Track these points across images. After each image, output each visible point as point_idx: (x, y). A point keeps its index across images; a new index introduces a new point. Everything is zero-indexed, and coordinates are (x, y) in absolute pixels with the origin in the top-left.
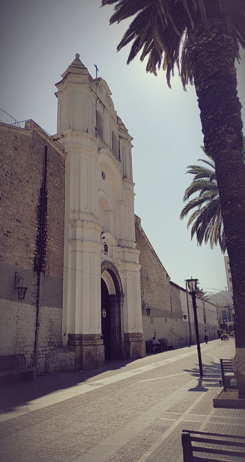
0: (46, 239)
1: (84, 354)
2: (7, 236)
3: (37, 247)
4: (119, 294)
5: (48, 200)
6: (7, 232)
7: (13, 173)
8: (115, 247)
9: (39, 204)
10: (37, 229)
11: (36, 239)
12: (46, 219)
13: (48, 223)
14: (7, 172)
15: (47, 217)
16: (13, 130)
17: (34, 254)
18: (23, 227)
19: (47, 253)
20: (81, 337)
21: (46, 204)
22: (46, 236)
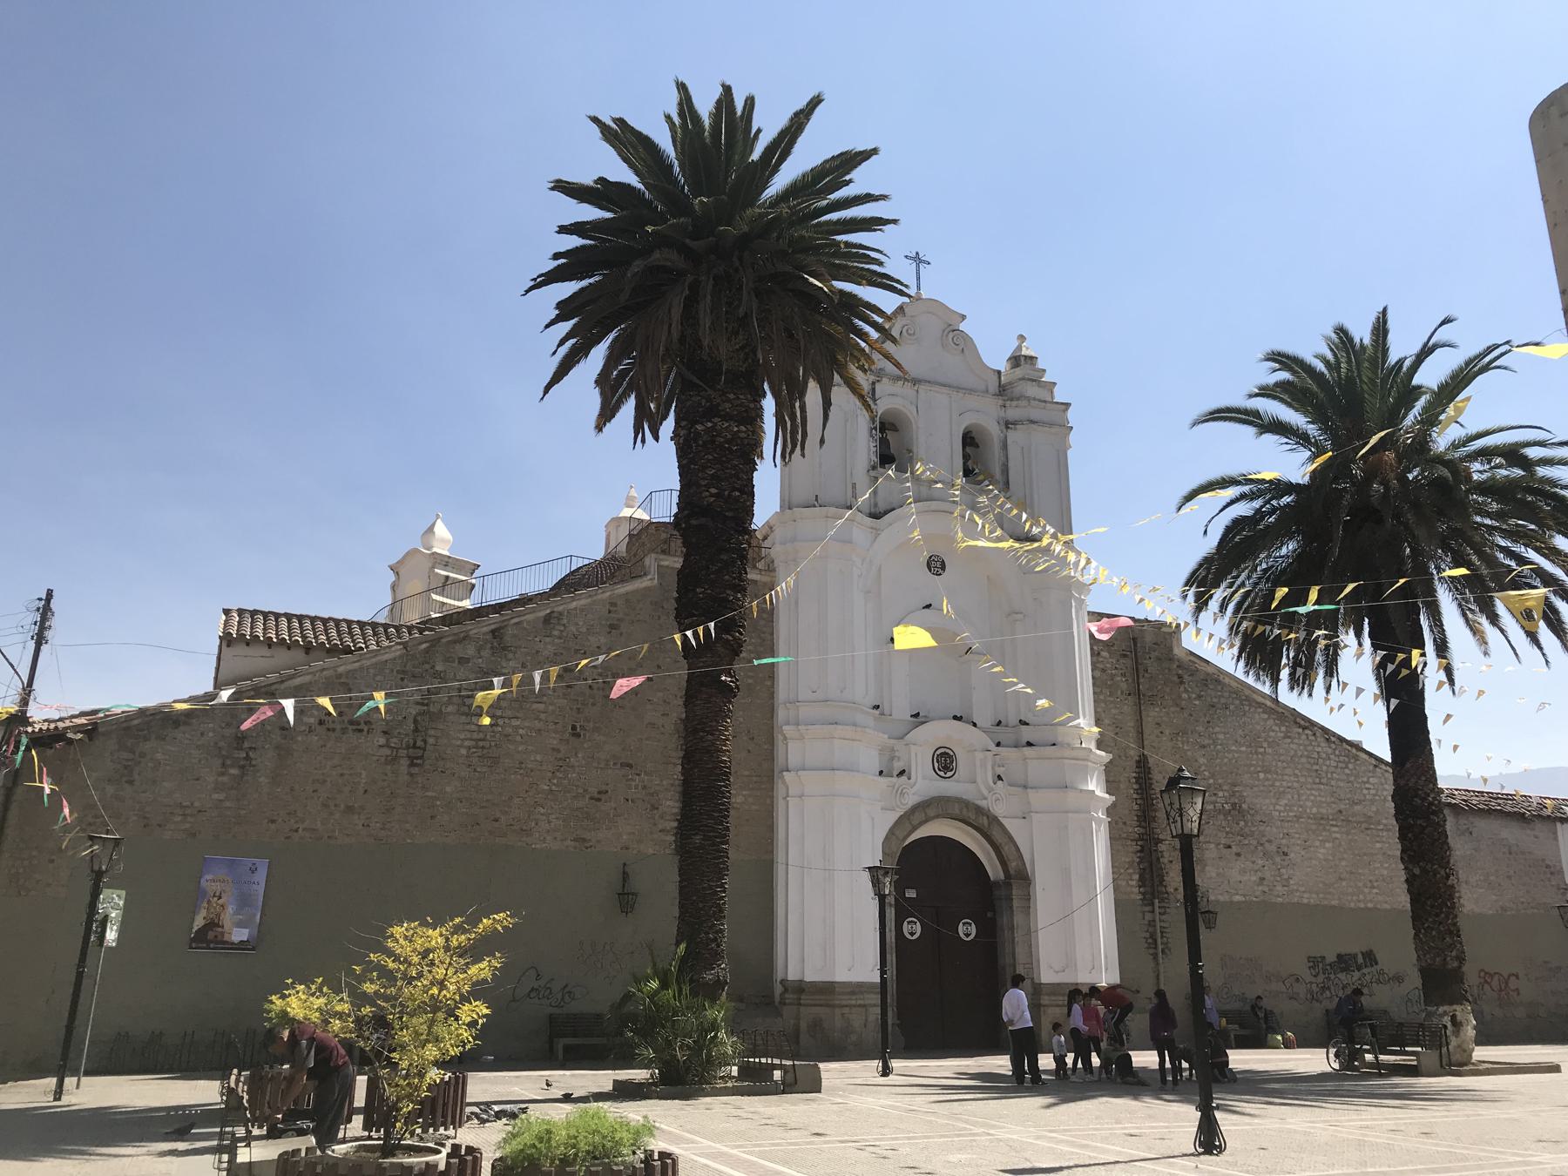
1: (803, 1025)
4: (1019, 877)
8: (979, 755)
11: (680, 789)
20: (801, 988)
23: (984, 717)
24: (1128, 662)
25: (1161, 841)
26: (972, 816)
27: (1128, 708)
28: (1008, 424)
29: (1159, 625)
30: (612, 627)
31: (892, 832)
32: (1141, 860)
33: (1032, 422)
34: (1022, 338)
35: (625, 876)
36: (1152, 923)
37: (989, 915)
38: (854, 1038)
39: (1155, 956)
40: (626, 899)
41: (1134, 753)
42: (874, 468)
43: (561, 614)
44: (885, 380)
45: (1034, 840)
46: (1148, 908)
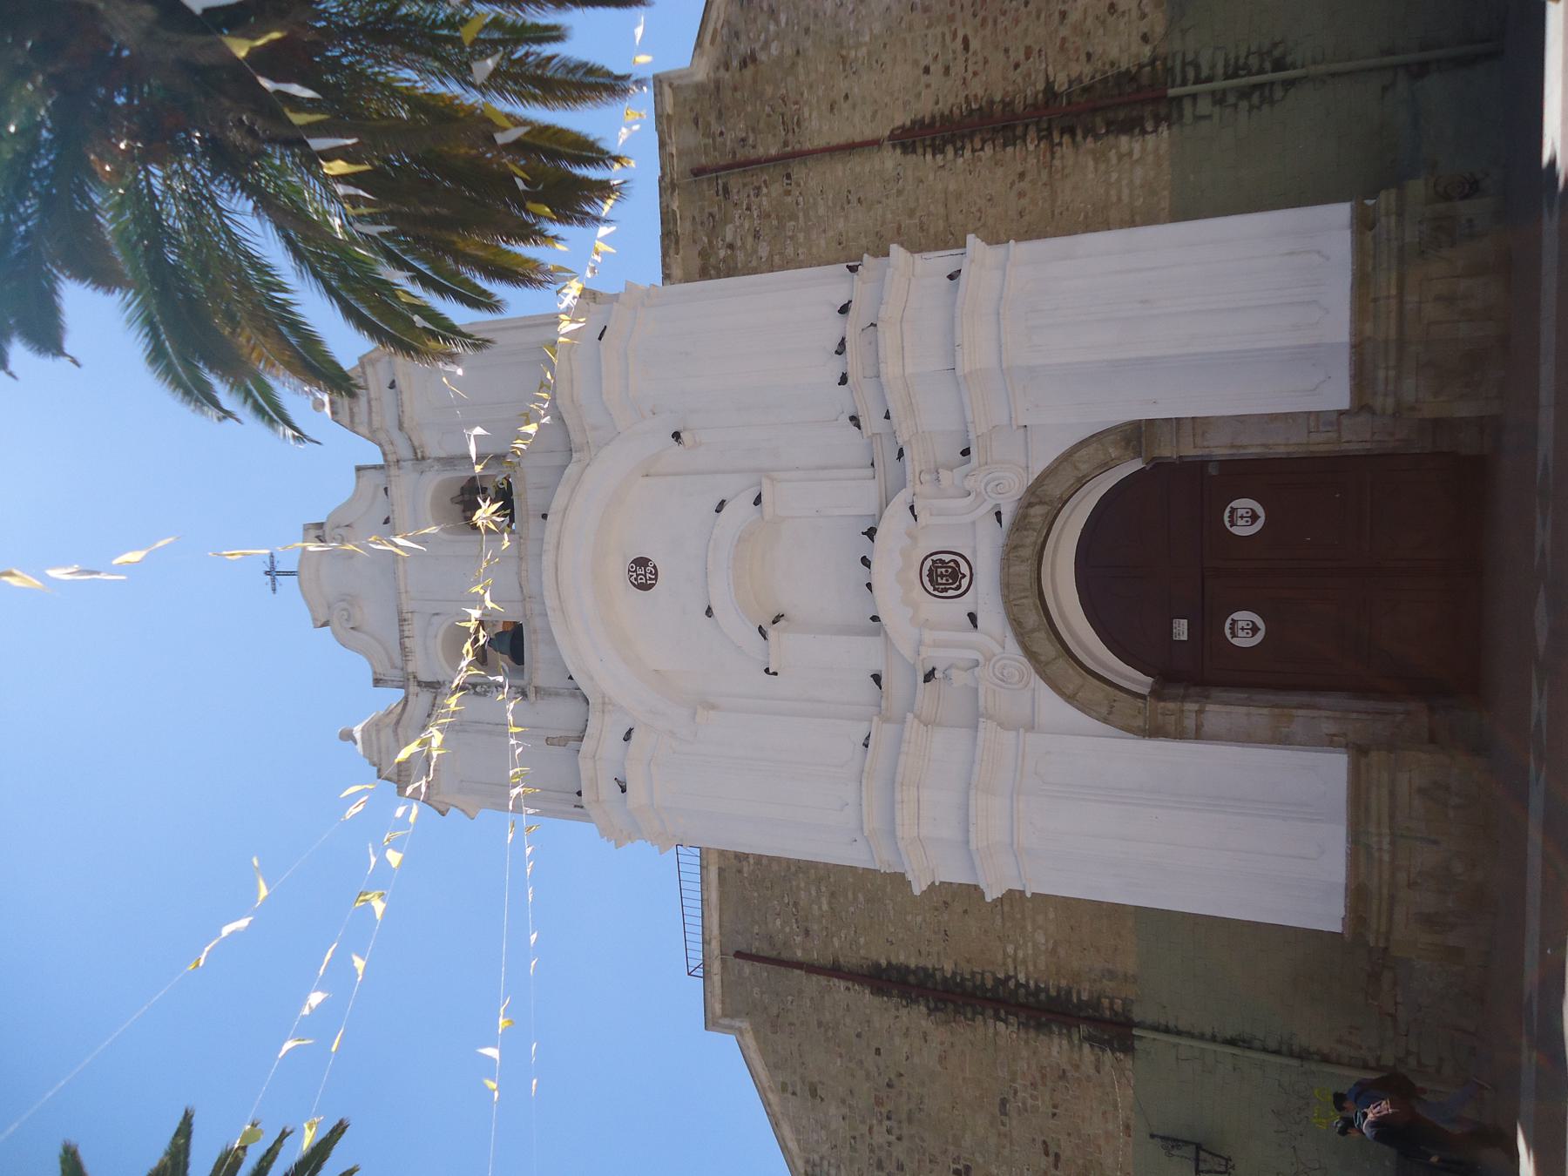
2: (1057, 1156)
3: (1055, 1029)
6: (1047, 1154)
9: (923, 1009)
10: (1001, 1026)
11: (1032, 1034)
12: (954, 974)
13: (966, 970)
14: (889, 1132)
15: (948, 968)
16: (776, 1108)
17: (1080, 1048)
18: (1016, 1093)
19: (1063, 983)
21: (907, 967)
22: (1012, 984)
23: (860, 497)
24: (735, 182)
25: (1049, 86)
26: (1031, 538)
27: (810, 177)
29: (663, 121)
30: (814, 1092)
31: (1070, 698)
32: (1090, 131)
33: (401, 427)
36: (1219, 98)
37: (1213, 470)
39: (1289, 84)
41: (890, 159)
43: (807, 1162)
44: (411, 668)
45: (1062, 422)
46: (1187, 106)
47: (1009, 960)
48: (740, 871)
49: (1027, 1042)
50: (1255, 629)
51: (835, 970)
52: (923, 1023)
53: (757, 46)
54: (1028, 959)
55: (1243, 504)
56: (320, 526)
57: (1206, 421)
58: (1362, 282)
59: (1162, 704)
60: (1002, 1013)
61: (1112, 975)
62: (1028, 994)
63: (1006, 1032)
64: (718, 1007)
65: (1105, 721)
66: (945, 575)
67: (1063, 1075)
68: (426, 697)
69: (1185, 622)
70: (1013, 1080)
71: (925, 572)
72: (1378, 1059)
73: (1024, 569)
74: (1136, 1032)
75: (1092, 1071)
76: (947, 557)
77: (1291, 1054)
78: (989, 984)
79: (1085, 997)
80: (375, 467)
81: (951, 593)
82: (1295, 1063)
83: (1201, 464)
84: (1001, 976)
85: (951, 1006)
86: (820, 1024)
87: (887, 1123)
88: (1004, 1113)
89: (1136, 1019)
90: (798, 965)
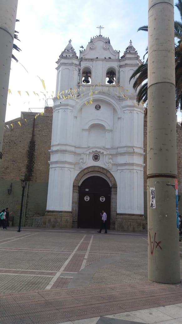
0: (34, 164)
2: (6, 169)
3: (27, 170)
4: (115, 186)
5: (36, 145)
6: (7, 167)
7: (11, 142)
9: (28, 149)
10: (27, 161)
14: (7, 142)
15: (36, 154)
17: (25, 173)
18: (16, 163)
19: (34, 171)
21: (34, 147)
22: (34, 163)
26: (101, 170)
28: (121, 66)
31: (78, 175)
33: (126, 64)
34: (131, 42)
35: (11, 186)
37: (109, 195)
38: (58, 224)
40: (10, 192)
42: (79, 83)
47: (37, 163)
48: (49, 120)
49: (25, 165)
50: (87, 200)
51: (33, 135)
52: (26, 149)
53: (178, 133)
54: (38, 166)
55: (104, 199)
56: (109, 42)
57: (117, 195)
58: (133, 215)
59: (77, 187)
60: (29, 162)
61: (36, 178)
62: (32, 166)
63: (26, 162)
64: (25, 114)
65: (75, 180)
66: (96, 158)
67: (20, 171)
68: (77, 63)
69: (88, 190)
70: (18, 163)
71: (97, 154)
72: (27, 214)
73: (97, 169)
74: (28, 182)
75: (21, 175)
76: (99, 158)
77: (27, 203)
78: (33, 160)
79: (33, 174)
80: (119, 56)
81: (93, 158)
82: (26, 203)
83: (110, 194)
84: (35, 162)
85: (29, 154)
86: (24, 132)
87: (8, 142)
88: (13, 161)
89: (30, 182)
90: (34, 129)
